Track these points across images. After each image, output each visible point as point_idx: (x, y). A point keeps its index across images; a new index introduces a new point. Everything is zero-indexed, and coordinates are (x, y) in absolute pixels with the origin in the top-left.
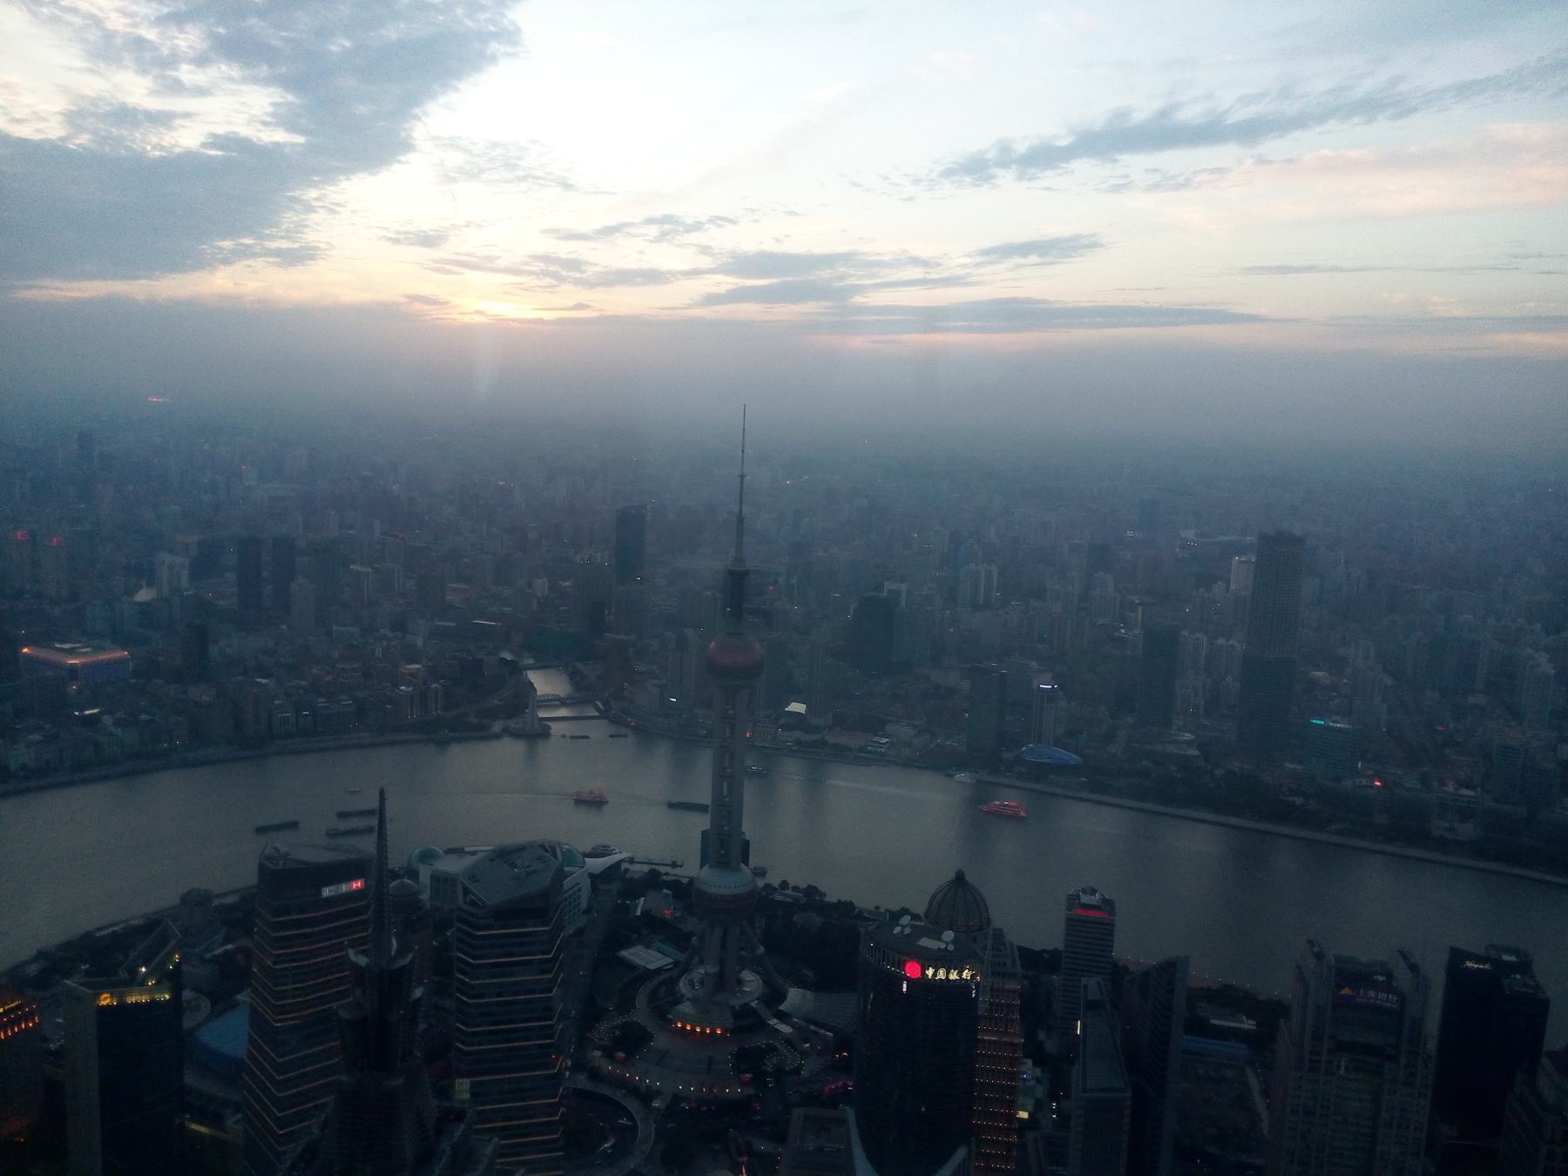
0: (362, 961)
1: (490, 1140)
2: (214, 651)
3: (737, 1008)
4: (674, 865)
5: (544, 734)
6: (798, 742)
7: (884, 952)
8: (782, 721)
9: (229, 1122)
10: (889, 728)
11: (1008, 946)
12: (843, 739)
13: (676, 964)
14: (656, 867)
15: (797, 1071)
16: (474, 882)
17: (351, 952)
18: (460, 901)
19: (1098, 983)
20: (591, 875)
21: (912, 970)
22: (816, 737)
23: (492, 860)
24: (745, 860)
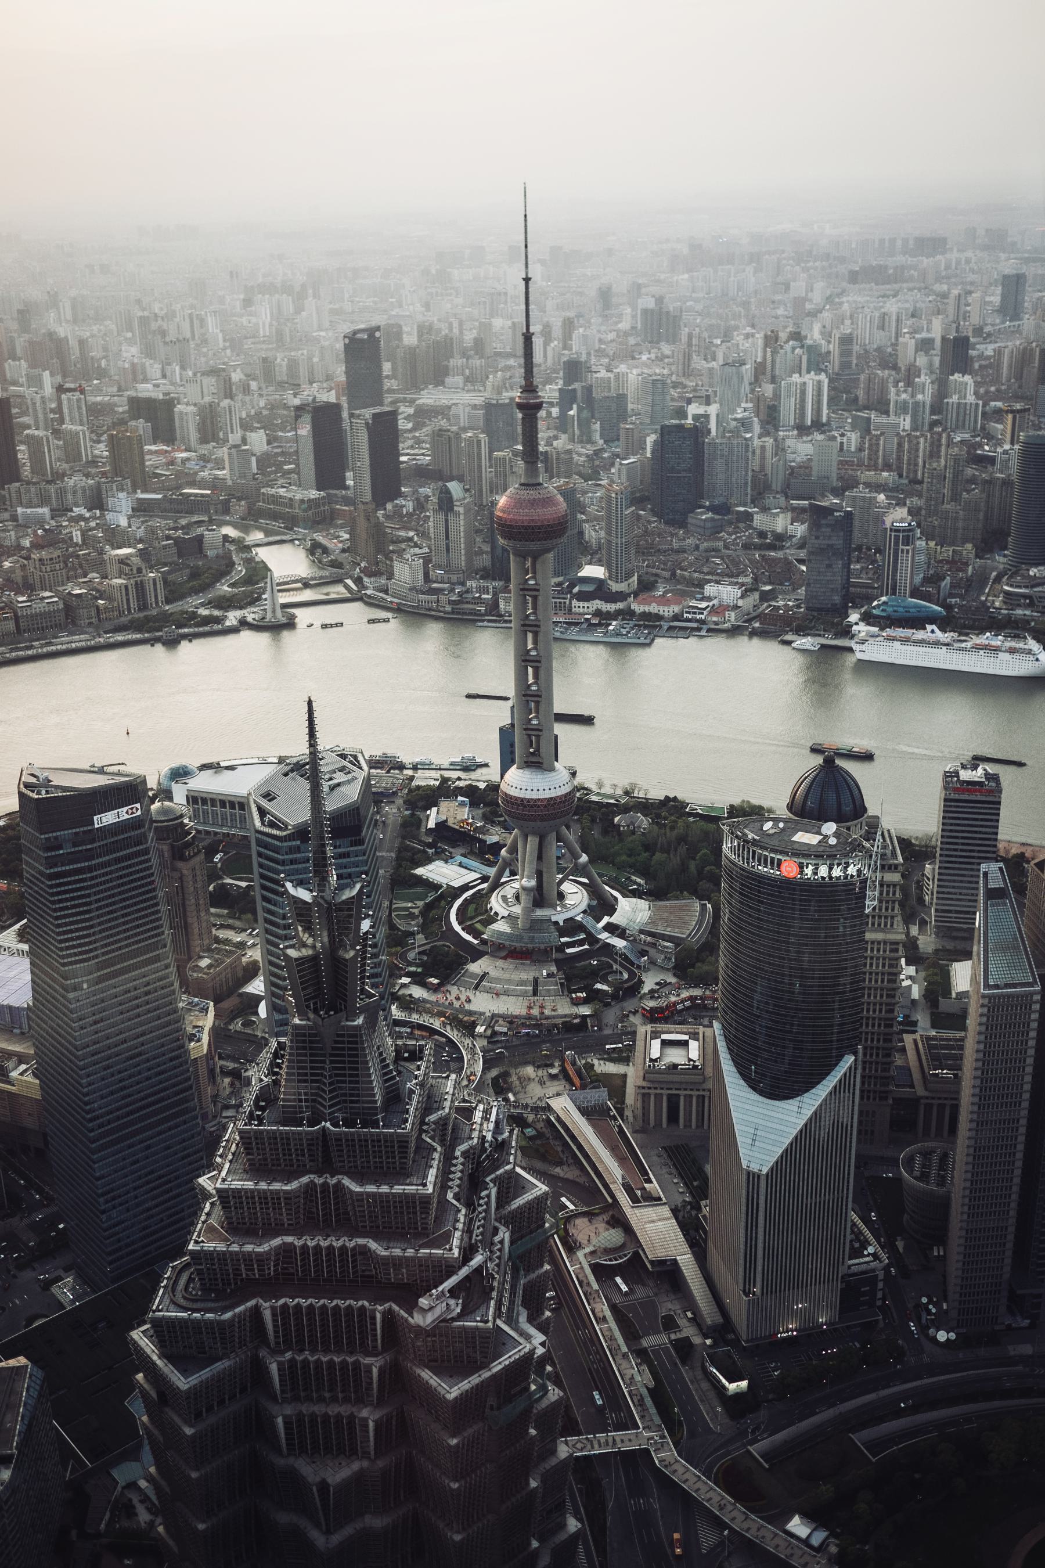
0: (304, 895)
1: (448, 1077)
3: (561, 924)
5: (290, 624)
6: (598, 613)
7: (754, 852)
8: (576, 590)
9: (14, 1074)
13: (484, 879)
14: (447, 774)
16: (270, 801)
17: (289, 885)
18: (258, 823)
19: (1001, 869)
22: (620, 605)
23: (286, 775)
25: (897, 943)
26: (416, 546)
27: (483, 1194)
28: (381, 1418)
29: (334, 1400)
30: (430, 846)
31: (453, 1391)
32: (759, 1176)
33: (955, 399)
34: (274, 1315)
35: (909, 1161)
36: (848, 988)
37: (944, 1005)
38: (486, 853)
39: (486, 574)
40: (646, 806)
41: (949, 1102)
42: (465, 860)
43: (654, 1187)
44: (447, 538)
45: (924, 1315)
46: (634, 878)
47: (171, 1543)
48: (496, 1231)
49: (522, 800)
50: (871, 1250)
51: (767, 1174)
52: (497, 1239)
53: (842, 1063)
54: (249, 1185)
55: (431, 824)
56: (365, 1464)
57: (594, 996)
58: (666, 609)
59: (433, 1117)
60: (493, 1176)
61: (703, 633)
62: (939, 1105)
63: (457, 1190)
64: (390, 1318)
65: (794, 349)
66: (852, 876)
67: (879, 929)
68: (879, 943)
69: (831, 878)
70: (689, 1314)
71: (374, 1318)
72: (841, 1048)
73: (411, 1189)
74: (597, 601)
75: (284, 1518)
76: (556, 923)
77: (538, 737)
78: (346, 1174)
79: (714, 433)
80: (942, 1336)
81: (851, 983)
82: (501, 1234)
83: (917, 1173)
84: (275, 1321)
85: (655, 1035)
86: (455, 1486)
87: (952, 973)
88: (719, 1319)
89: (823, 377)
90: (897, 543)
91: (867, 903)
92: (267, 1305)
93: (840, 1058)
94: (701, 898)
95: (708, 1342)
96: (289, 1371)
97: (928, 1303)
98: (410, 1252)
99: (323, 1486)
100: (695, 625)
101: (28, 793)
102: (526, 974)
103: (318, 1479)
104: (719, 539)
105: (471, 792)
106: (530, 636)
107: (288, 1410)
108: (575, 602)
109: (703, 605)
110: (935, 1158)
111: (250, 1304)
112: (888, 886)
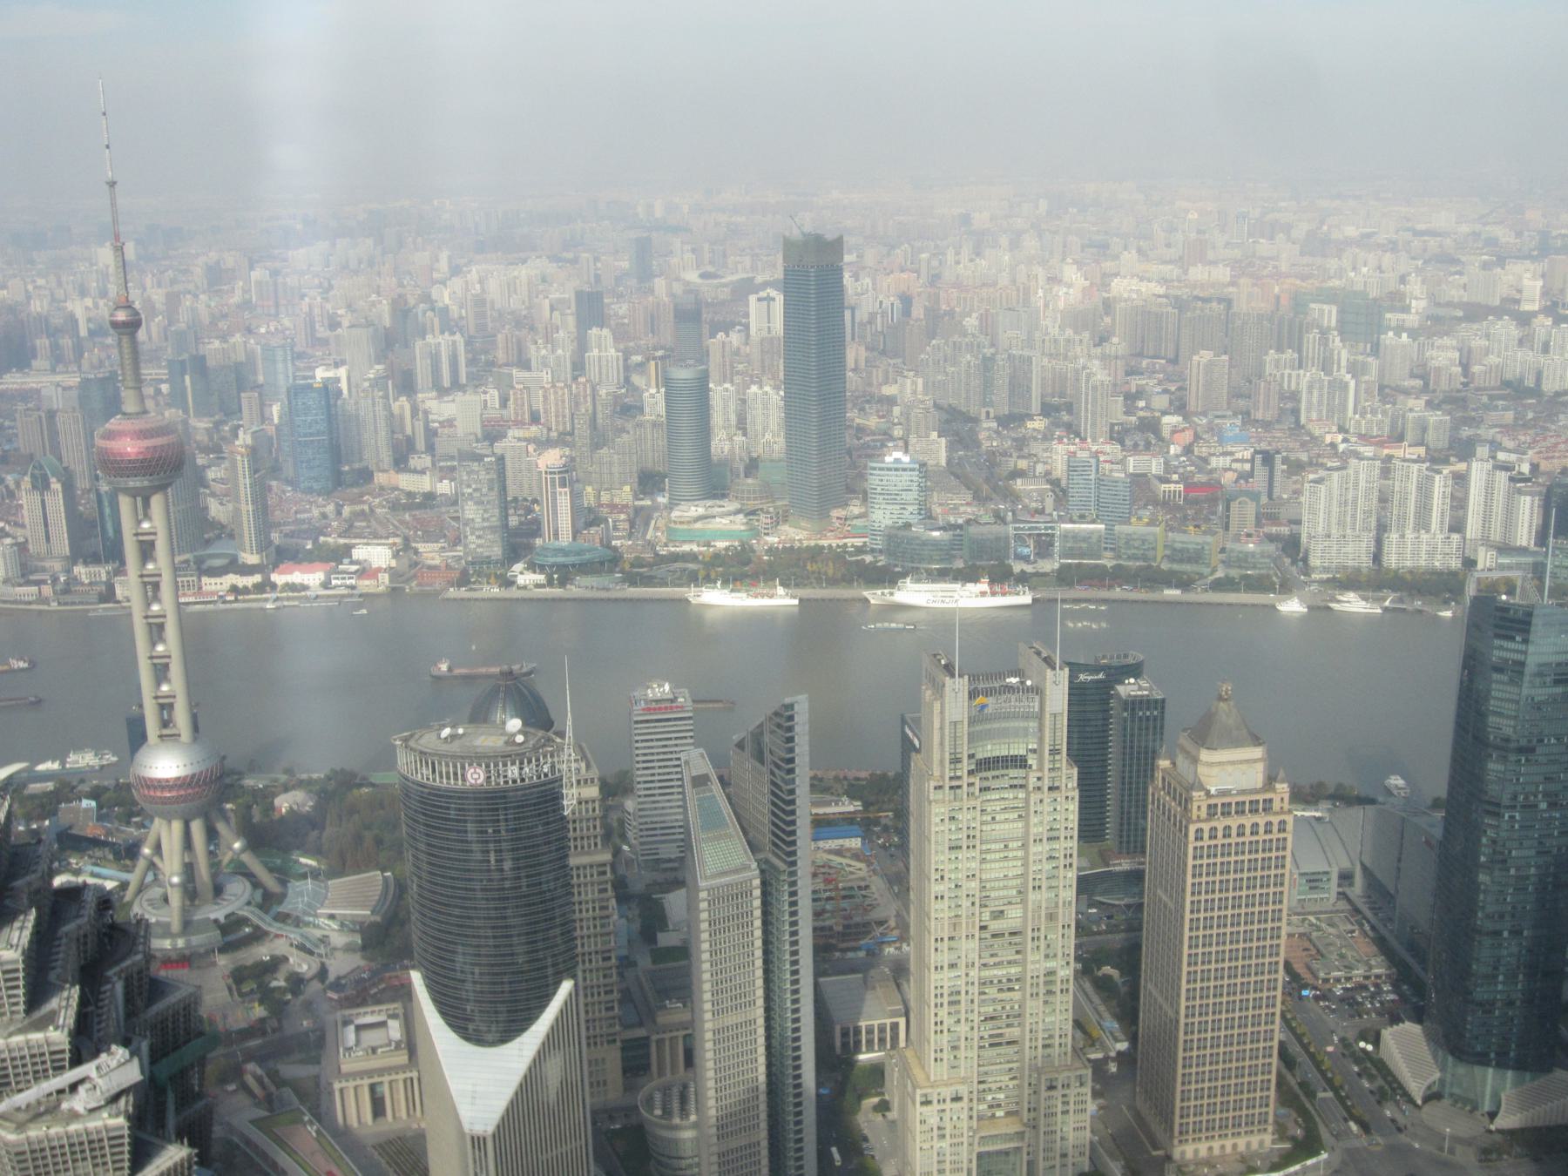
3: (222, 920)
6: (234, 589)
8: (205, 566)
10: (359, 553)
12: (297, 577)
13: (124, 886)
21: (476, 776)
22: (257, 578)
25: (604, 865)
26: (7, 535)
27: (109, 987)
32: (484, 1139)
33: (596, 352)
36: (559, 940)
37: (665, 940)
39: (93, 559)
41: (683, 1033)
42: (97, 870)
44: (46, 525)
46: (303, 860)
51: (494, 1136)
58: (311, 576)
60: (116, 969)
62: (671, 1039)
65: (424, 313)
66: (546, 775)
67: (583, 853)
68: (585, 868)
69: (523, 780)
72: (558, 973)
76: (216, 921)
79: (345, 391)
81: (562, 934)
83: (658, 1112)
85: (346, 1023)
87: (666, 905)
89: (458, 337)
90: (553, 486)
91: (565, 803)
93: (557, 984)
104: (364, 502)
106: (149, 588)
108: (205, 580)
109: (354, 568)
110: (675, 1091)
112: (587, 802)
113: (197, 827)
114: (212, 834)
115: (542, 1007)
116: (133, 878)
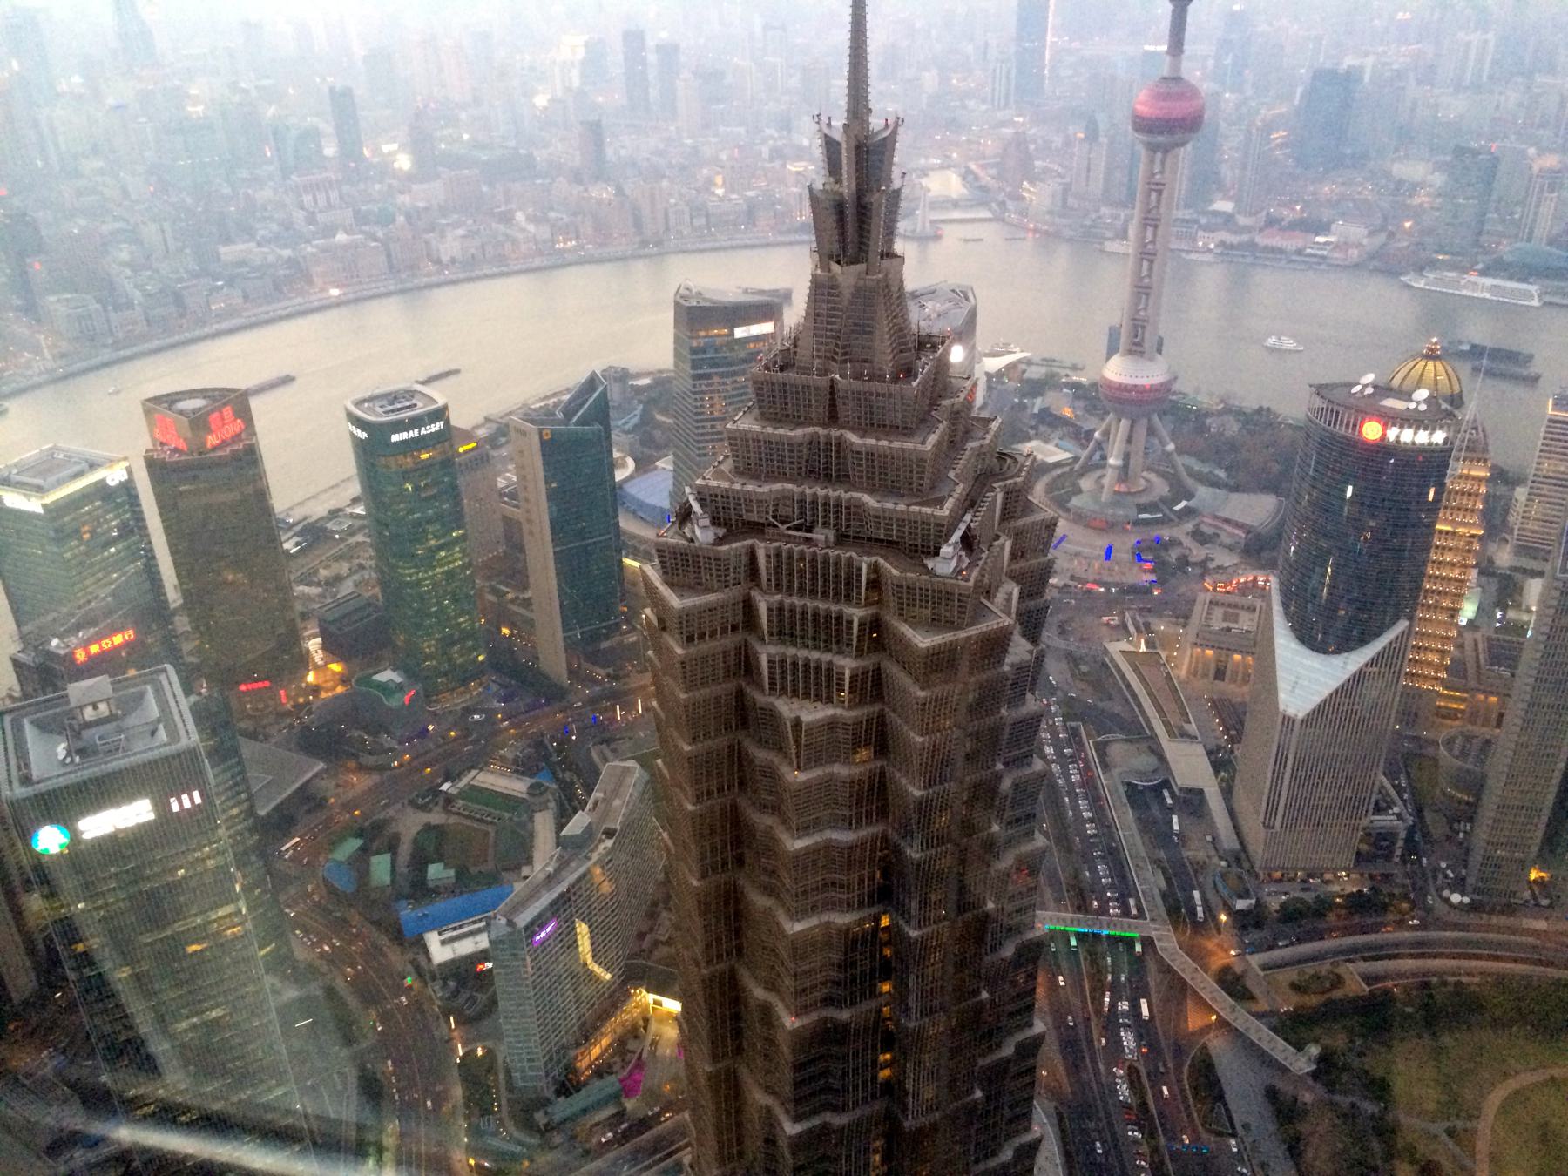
2: (610, 152)
4: (1075, 368)
5: (937, 237)
6: (1222, 244)
11: (1480, 429)
13: (1076, 459)
15: (1203, 564)
20: (987, 374)
21: (1371, 431)
22: (1245, 238)
24: (1159, 351)
28: (857, 668)
29: (816, 648)
30: (1032, 427)
31: (924, 641)
34: (768, 556)
35: (1450, 742)
38: (1081, 436)
40: (1239, 413)
42: (1060, 442)
43: (1192, 728)
45: (1440, 876)
47: (666, 772)
48: (997, 537)
49: (1120, 384)
50: (1396, 810)
52: (996, 543)
53: (1395, 627)
54: (756, 428)
55: (1036, 411)
56: (839, 711)
57: (1160, 567)
59: (945, 402)
60: (1001, 484)
61: (1323, 267)
63: (958, 471)
64: (875, 568)
70: (1209, 838)
71: (860, 569)
73: (909, 445)
74: (1223, 233)
75: (761, 755)
77: (1143, 327)
78: (852, 430)
80: (1456, 898)
82: (1002, 540)
83: (1457, 752)
84: (768, 562)
86: (920, 739)
88: (1237, 846)
92: (762, 545)
93: (1393, 622)
94: (1278, 495)
95: (1223, 863)
96: (778, 612)
97: (1448, 868)
98: (901, 507)
99: (797, 723)
100: (1315, 260)
101: (682, 301)
102: (1102, 542)
103: (793, 716)
105: (1076, 386)
107: (773, 650)
111: (748, 542)
113: (1141, 431)
114: (1151, 431)
115: (1378, 635)
116: (1084, 454)
